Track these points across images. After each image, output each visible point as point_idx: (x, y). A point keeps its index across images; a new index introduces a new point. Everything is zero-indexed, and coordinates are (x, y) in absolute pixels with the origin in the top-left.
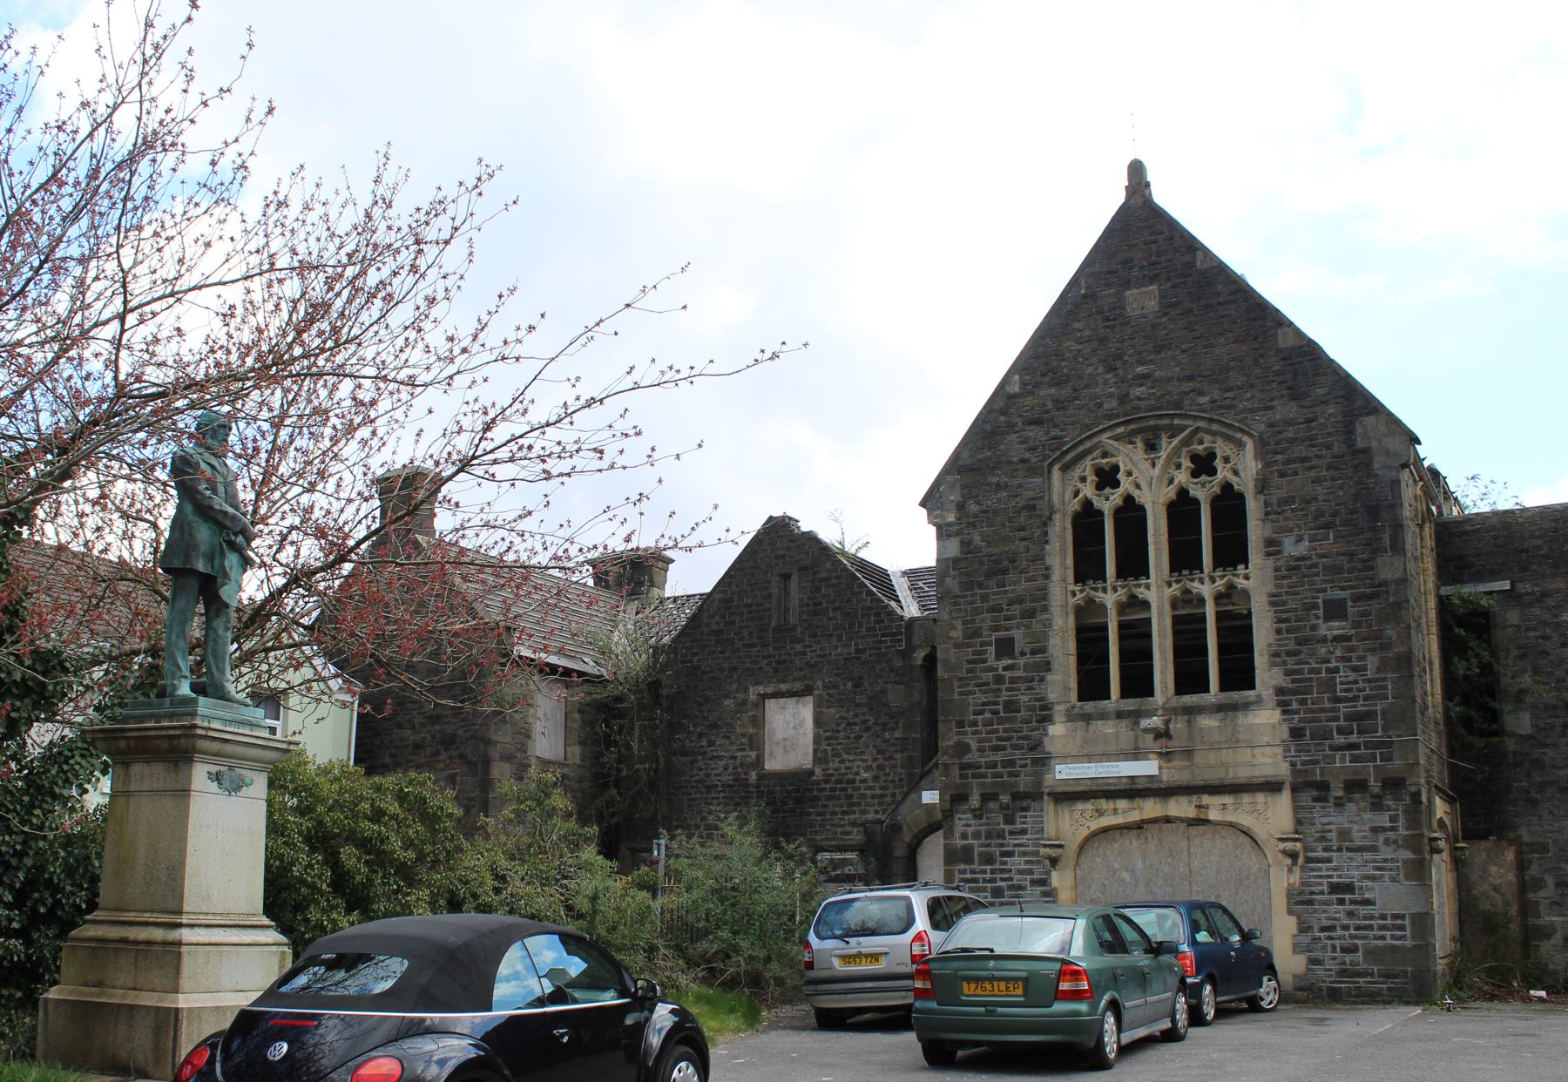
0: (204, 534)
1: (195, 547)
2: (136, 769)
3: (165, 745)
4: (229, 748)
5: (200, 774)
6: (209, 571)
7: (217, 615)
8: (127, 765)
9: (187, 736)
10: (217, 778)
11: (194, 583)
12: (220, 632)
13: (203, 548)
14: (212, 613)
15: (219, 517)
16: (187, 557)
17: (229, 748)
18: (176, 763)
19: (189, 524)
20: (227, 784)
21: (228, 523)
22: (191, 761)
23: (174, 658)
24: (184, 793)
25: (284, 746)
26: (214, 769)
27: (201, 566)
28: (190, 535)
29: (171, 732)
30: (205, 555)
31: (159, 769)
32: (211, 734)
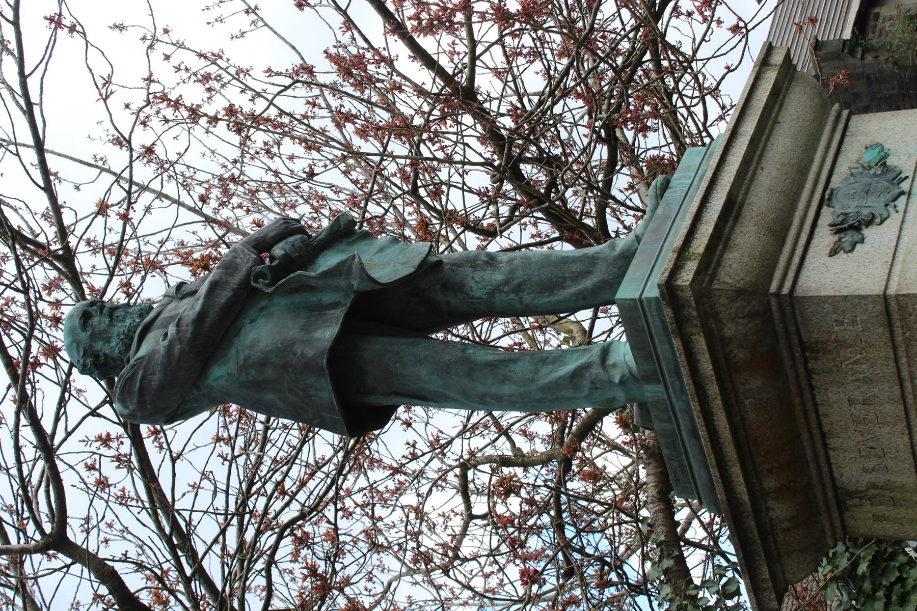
0: (262, 334)
1: (285, 349)
2: (851, 471)
3: (753, 385)
4: (762, 199)
5: (831, 273)
6: (339, 314)
7: (459, 288)
8: (843, 498)
9: (710, 320)
10: (851, 229)
11: (378, 349)
12: (498, 277)
13: (293, 330)
14: (455, 301)
15: (223, 297)
16: (308, 367)
17: (762, 199)
18: (809, 350)
19: (244, 367)
20: (875, 204)
21: (236, 280)
22: (792, 303)
23: (557, 384)
24: (891, 310)
25: (771, 77)
26: (824, 238)
27: (327, 333)
28: (262, 363)
29: (706, 366)
30: (307, 328)
31: (837, 401)
32: (700, 245)
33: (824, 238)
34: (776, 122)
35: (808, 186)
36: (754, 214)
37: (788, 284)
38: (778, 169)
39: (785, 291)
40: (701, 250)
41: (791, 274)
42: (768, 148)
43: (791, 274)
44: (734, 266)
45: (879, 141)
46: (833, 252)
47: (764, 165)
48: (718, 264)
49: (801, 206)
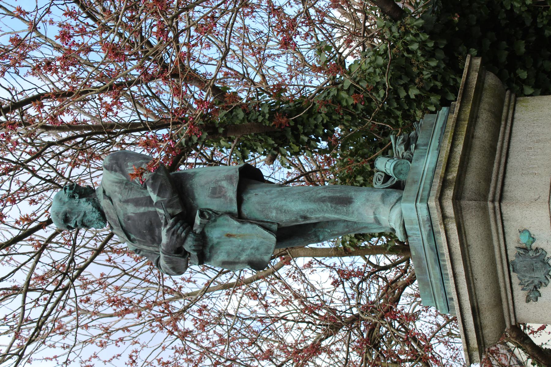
4: (485, 297)
17: (485, 297)
33: (520, 295)
34: (468, 246)
35: (499, 267)
36: (485, 306)
37: (513, 320)
38: (484, 275)
39: (513, 324)
40: (476, 346)
41: (512, 315)
42: (473, 265)
43: (512, 315)
44: (490, 335)
45: (526, 226)
46: (528, 301)
47: (476, 277)
48: (483, 337)
49: (501, 280)
